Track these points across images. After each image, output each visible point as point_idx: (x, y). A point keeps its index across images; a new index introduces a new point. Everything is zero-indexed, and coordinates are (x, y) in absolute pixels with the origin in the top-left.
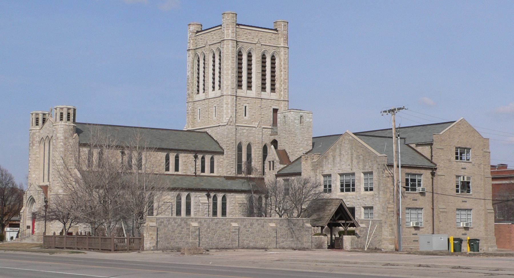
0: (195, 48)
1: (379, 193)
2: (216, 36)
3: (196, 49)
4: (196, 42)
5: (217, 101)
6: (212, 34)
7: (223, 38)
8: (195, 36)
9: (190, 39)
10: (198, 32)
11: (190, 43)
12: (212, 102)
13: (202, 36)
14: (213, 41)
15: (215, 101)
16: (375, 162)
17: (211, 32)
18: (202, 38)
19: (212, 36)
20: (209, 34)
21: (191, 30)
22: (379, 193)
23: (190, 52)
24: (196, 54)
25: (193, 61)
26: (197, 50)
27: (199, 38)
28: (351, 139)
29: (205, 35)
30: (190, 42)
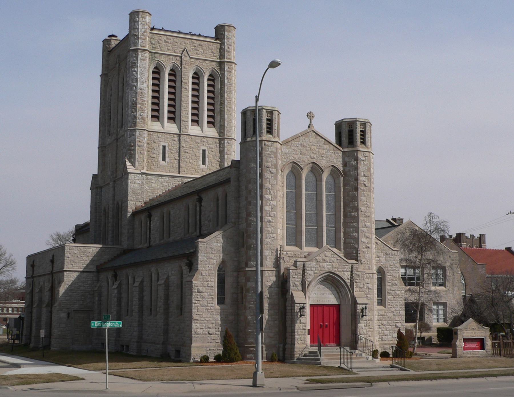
0: (153, 51)
1: (453, 289)
2: (203, 49)
3: (155, 53)
4: (153, 42)
5: (211, 142)
6: (194, 43)
7: (230, 59)
8: (150, 33)
9: (145, 34)
10: (152, 29)
11: (144, 39)
12: (199, 141)
13: (168, 39)
14: (198, 54)
15: (204, 142)
16: (448, 257)
17: (193, 41)
18: (169, 41)
19: (195, 46)
20: (186, 41)
21: (147, 21)
22: (453, 289)
23: (147, 54)
24: (151, 59)
25: (149, 70)
26: (156, 55)
27: (161, 38)
28: (418, 229)
29: (177, 40)
30: (146, 38)
